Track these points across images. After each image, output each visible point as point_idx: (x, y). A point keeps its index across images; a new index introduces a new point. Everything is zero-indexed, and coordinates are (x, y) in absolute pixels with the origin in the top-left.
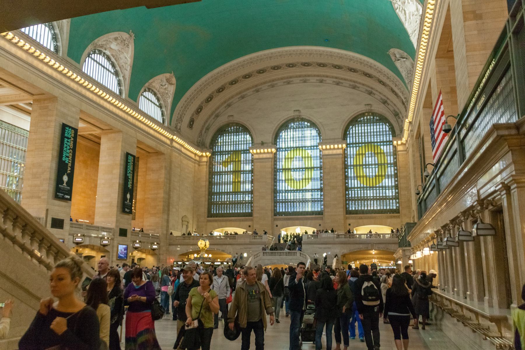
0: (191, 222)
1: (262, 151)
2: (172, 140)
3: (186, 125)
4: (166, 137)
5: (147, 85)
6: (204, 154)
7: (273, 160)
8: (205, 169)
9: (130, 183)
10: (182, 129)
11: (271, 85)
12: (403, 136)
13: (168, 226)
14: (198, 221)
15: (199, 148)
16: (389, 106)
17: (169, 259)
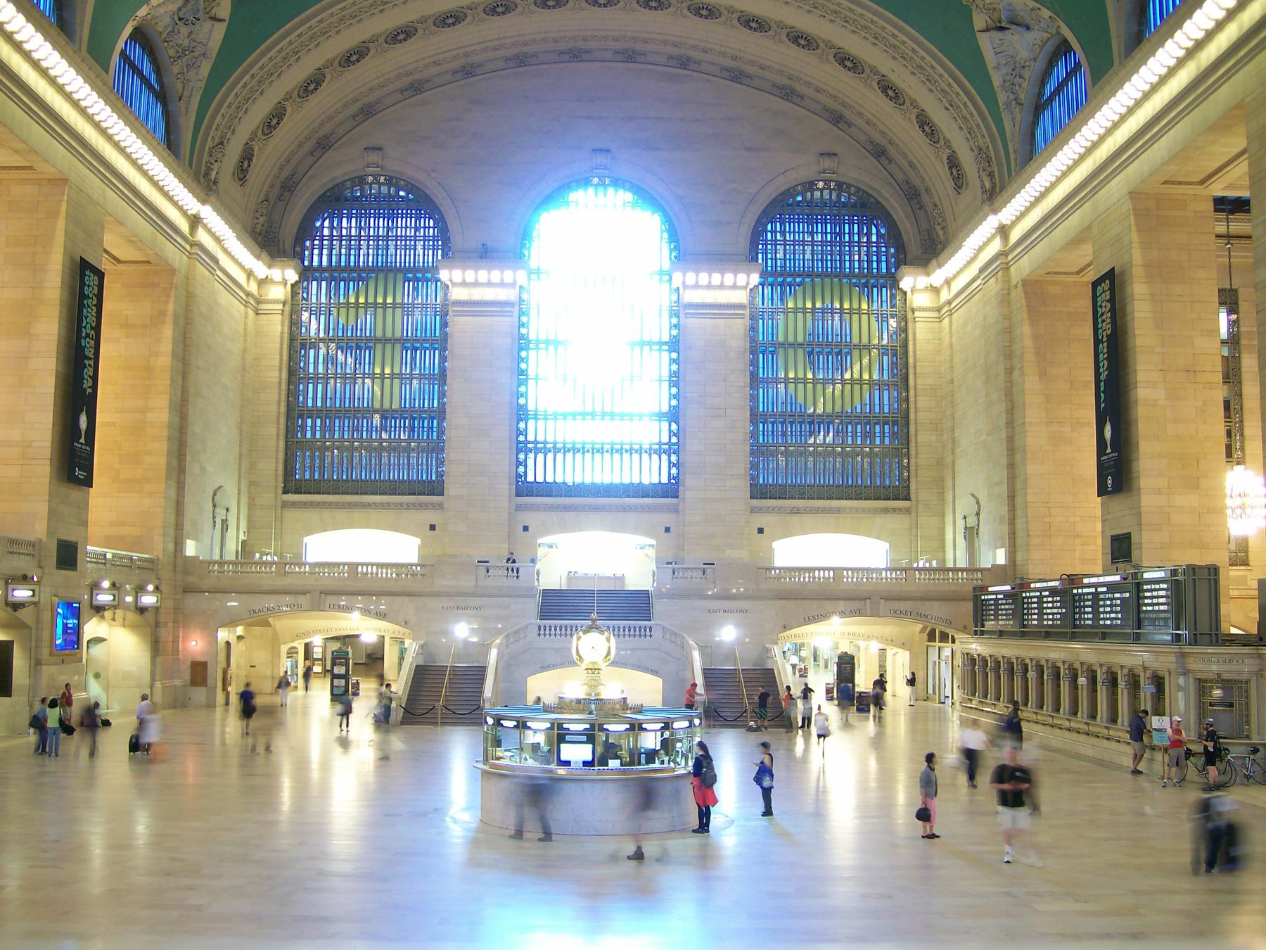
0: (234, 510)
1: (483, 275)
2: (195, 221)
3: (232, 170)
4: (180, 208)
5: (142, 12)
6: (276, 274)
7: (516, 310)
8: (279, 329)
9: (89, 371)
10: (221, 185)
11: (517, 56)
12: (940, 266)
13: (179, 527)
14: (251, 505)
15: (264, 255)
16: (892, 168)
17: (185, 639)
